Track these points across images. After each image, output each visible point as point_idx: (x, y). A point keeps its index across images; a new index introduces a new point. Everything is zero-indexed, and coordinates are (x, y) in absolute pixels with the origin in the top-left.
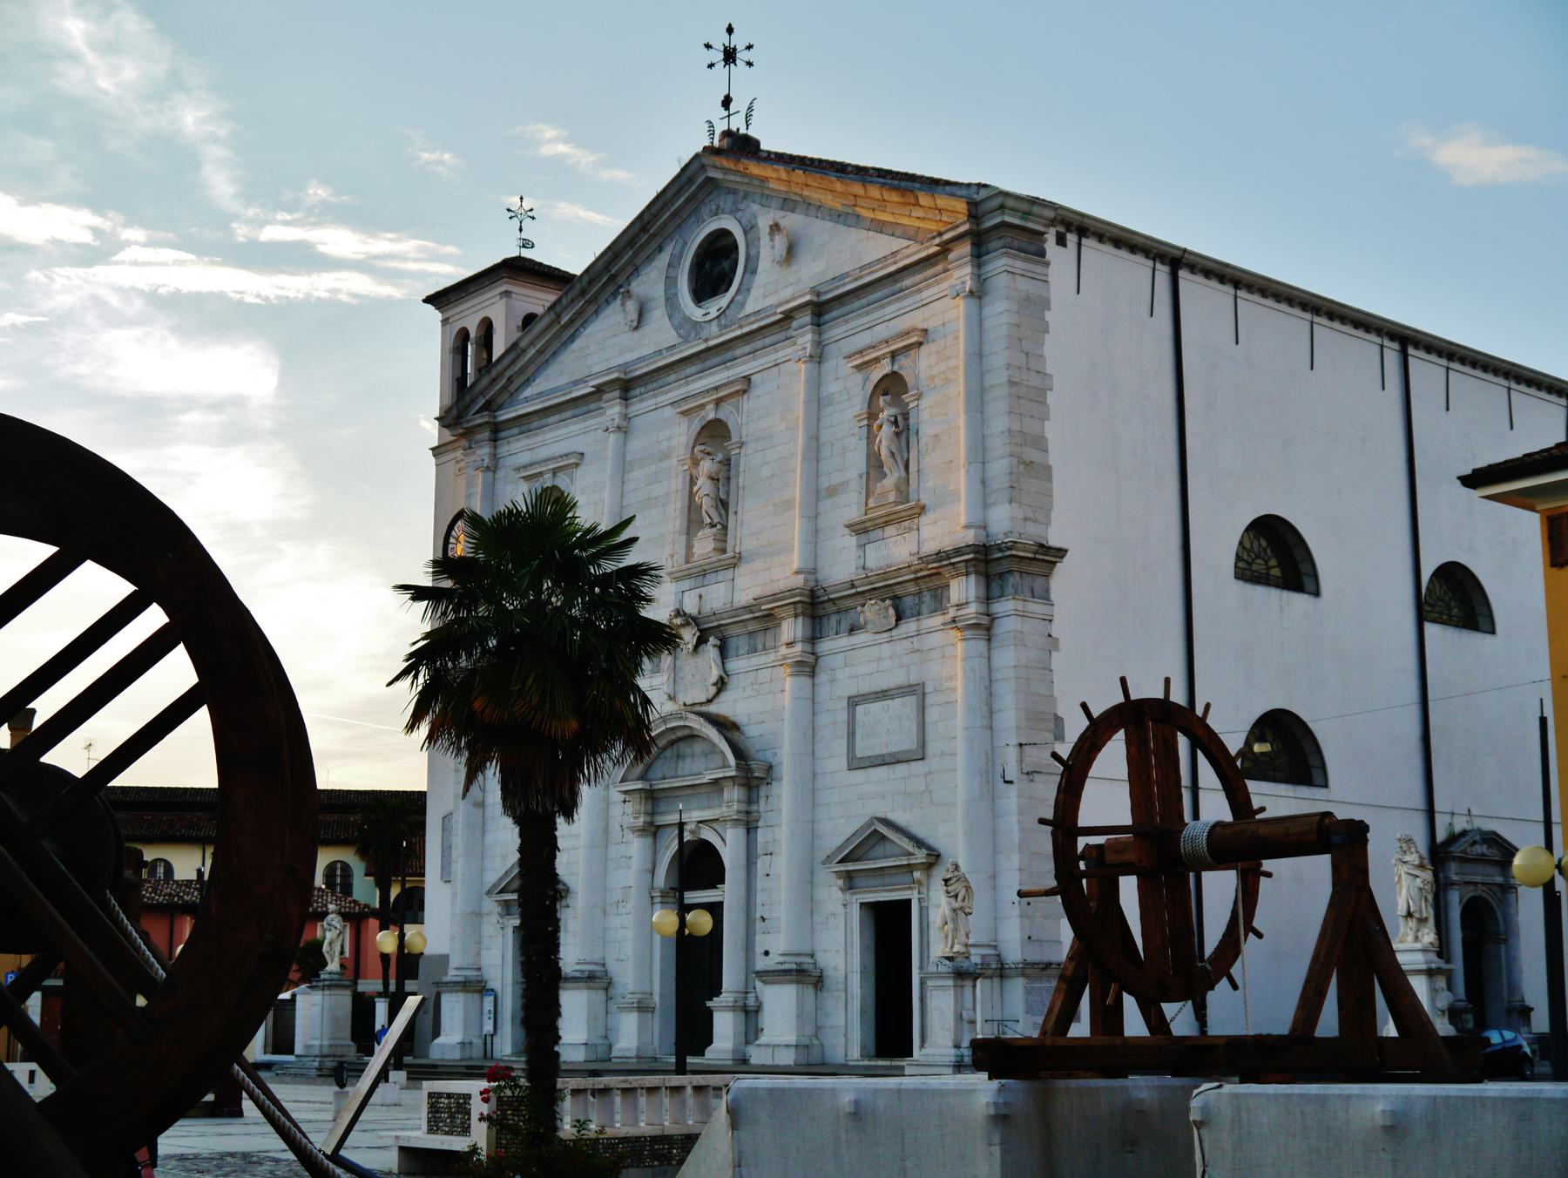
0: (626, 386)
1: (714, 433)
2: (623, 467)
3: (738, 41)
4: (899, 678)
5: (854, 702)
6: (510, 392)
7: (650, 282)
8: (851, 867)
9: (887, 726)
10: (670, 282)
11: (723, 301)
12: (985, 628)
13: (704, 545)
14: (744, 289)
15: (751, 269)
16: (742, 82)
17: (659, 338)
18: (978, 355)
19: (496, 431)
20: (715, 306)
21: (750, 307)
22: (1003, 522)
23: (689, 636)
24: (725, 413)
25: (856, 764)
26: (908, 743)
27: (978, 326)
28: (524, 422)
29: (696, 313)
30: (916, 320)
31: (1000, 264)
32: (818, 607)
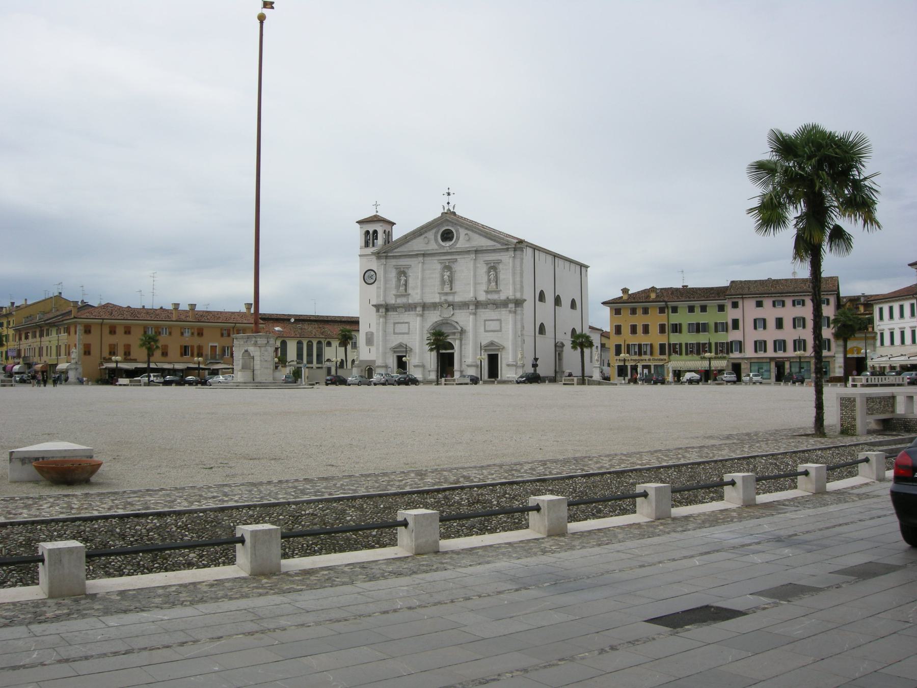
0: (424, 255)
1: (448, 268)
2: (423, 270)
3: (451, 192)
4: (495, 318)
5: (485, 321)
6: (391, 250)
7: (430, 235)
8: (195, 353)
9: (493, 325)
10: (436, 237)
11: (451, 243)
12: (515, 312)
13: (447, 289)
14: (456, 242)
15: (458, 239)
16: (452, 199)
17: (433, 247)
18: (514, 267)
19: (387, 257)
20: (448, 244)
21: (458, 246)
22: (518, 296)
23: (446, 305)
24: (451, 264)
25: (486, 331)
26: (498, 328)
27: (514, 262)
28: (394, 257)
29: (443, 244)
30: (500, 258)
31: (518, 253)
32: (478, 304)
